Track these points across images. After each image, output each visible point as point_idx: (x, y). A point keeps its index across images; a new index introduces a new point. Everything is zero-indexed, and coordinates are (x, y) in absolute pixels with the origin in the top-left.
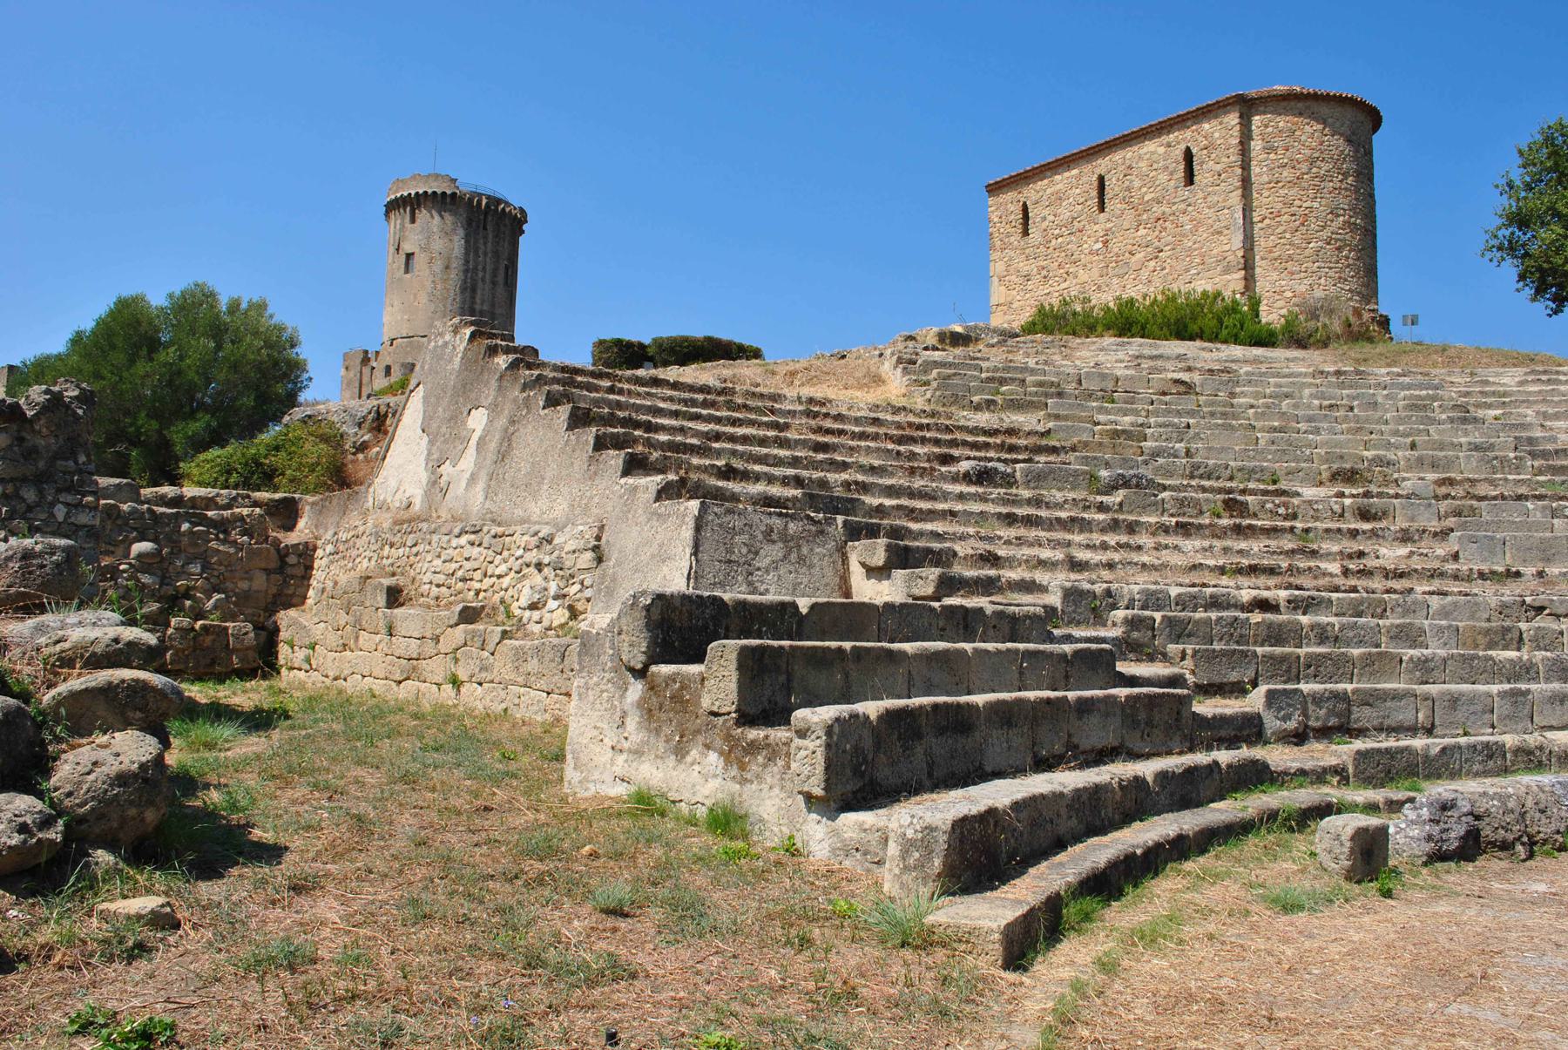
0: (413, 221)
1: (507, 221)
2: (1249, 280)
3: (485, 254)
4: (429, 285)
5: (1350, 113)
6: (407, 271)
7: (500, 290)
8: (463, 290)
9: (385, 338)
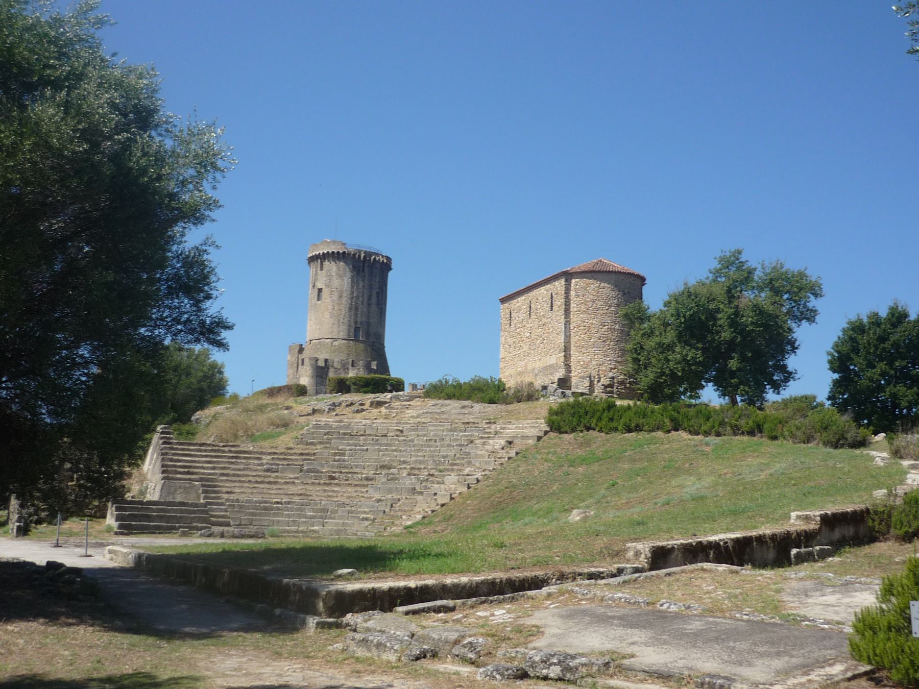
0: (322, 269)
1: (378, 265)
2: (567, 357)
3: (364, 287)
4: (330, 308)
5: (614, 276)
6: (318, 300)
7: (374, 308)
8: (350, 309)
9: (308, 340)
